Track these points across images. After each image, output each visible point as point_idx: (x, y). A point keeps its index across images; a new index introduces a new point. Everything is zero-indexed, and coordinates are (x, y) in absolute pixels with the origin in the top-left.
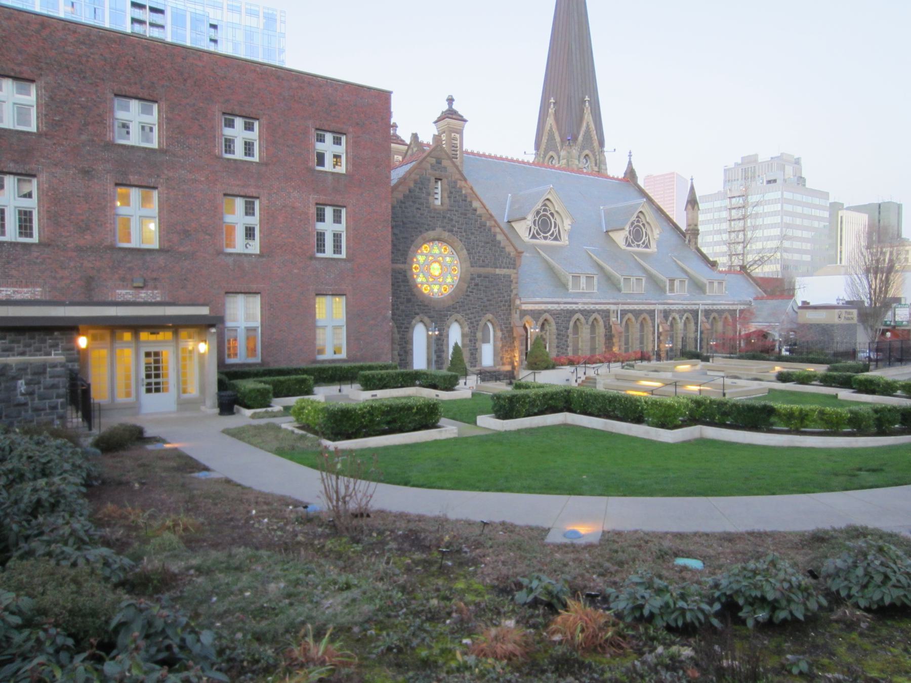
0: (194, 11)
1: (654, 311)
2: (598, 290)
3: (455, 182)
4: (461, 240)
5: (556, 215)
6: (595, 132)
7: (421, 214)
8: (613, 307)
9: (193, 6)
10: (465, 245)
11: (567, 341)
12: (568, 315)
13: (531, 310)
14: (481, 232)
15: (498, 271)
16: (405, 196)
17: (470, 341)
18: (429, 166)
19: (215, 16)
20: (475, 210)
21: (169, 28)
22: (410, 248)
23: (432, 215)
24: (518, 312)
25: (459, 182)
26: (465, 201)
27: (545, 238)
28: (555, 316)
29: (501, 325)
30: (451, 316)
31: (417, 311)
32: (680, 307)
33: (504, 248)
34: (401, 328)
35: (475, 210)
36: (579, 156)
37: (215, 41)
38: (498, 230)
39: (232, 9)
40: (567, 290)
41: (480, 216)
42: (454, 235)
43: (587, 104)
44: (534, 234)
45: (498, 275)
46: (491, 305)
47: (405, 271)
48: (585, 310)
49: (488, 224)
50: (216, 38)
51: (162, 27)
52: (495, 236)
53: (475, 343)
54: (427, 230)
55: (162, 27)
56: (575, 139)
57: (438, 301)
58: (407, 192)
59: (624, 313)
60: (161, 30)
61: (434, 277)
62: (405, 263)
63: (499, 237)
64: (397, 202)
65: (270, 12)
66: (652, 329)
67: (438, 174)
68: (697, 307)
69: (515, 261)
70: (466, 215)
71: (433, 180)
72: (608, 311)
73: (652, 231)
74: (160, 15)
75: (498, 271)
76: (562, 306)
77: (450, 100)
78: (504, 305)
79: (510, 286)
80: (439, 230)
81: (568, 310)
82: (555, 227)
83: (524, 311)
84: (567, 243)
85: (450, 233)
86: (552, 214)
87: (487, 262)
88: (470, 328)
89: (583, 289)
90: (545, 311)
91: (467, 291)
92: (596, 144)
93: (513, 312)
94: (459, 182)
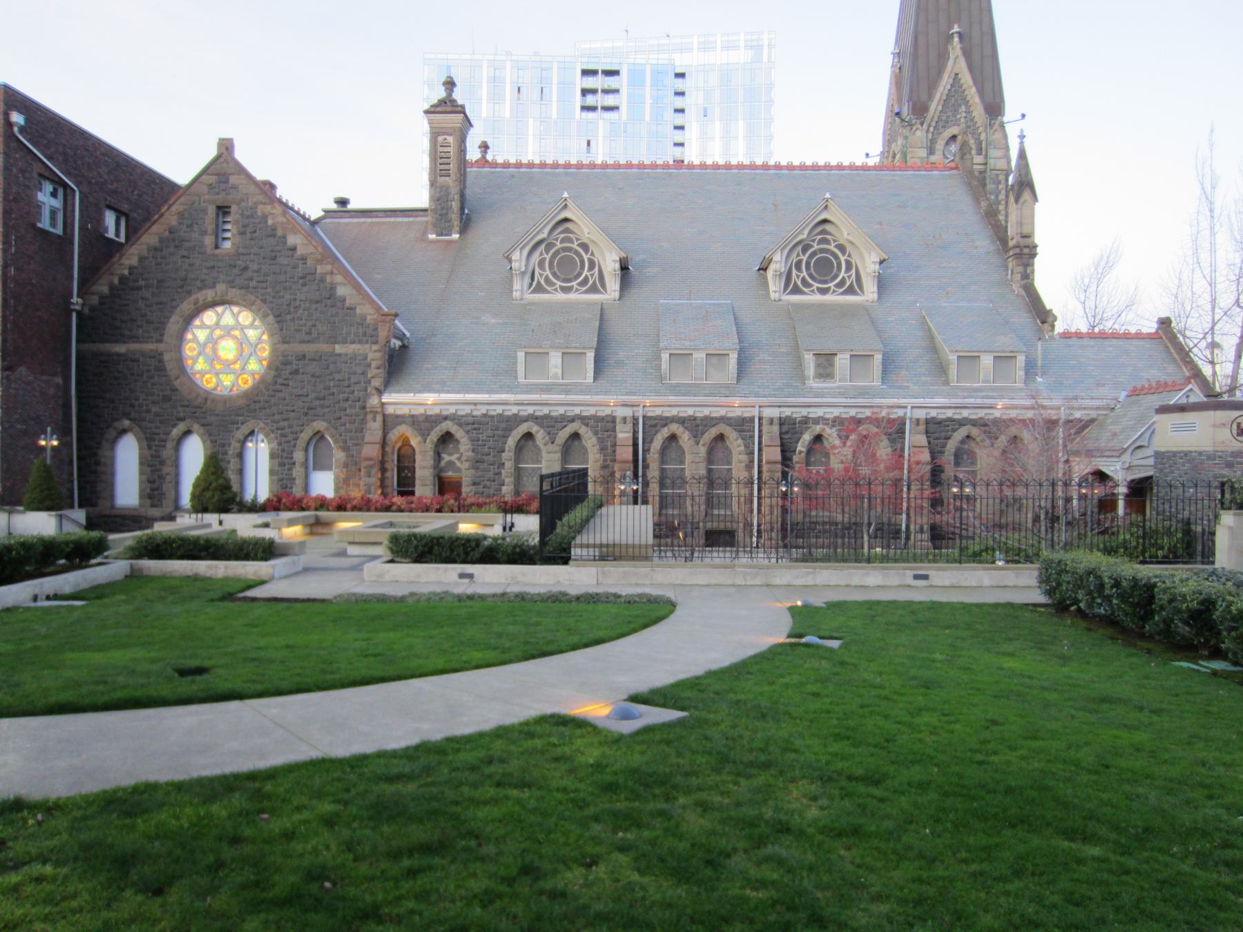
0: (655, 62)
1: (752, 419)
2: (595, 378)
3: (254, 208)
4: (264, 301)
6: (974, 90)
7: (190, 265)
8: (621, 412)
9: (656, 56)
10: (271, 310)
11: (500, 474)
12: (502, 425)
13: (413, 416)
14: (304, 285)
15: (339, 349)
16: (161, 240)
17: (281, 465)
18: (205, 189)
19: (680, 65)
20: (294, 249)
21: (624, 92)
22: (169, 318)
23: (211, 264)
24: (379, 418)
25: (260, 207)
26: (274, 236)
27: (566, 290)
28: (469, 427)
30: (243, 423)
31: (182, 415)
32: (836, 412)
33: (352, 309)
34: (153, 440)
35: (294, 249)
36: (933, 142)
37: (681, 94)
38: (339, 278)
39: (706, 47)
40: (516, 378)
41: (303, 259)
42: (251, 293)
43: (956, 39)
44: (538, 282)
45: (340, 355)
46: (322, 406)
47: (161, 354)
48: (546, 417)
49: (320, 269)
50: (684, 90)
51: (616, 91)
52: (333, 288)
53: (290, 469)
54: (201, 289)
55: (616, 91)
56: (920, 110)
57: (226, 400)
58: (167, 233)
59: (654, 424)
60: (616, 96)
61: (227, 364)
62: (160, 341)
63: (341, 291)
64: (149, 250)
65: (755, 37)
66: (744, 457)
67: (221, 199)
68: (900, 413)
69: (376, 329)
70: (274, 258)
71: (211, 210)
72: (612, 420)
73: (863, 259)
74: (616, 78)
75: (339, 349)
76: (482, 410)
77: (450, 84)
78: (350, 406)
79: (364, 373)
80: (221, 287)
81: (500, 415)
83: (398, 416)
84: (617, 295)
85: (243, 291)
87: (315, 335)
88: (280, 444)
89: (556, 376)
90: (446, 418)
91: (276, 383)
92: (978, 112)
93: (369, 417)
94: (260, 207)
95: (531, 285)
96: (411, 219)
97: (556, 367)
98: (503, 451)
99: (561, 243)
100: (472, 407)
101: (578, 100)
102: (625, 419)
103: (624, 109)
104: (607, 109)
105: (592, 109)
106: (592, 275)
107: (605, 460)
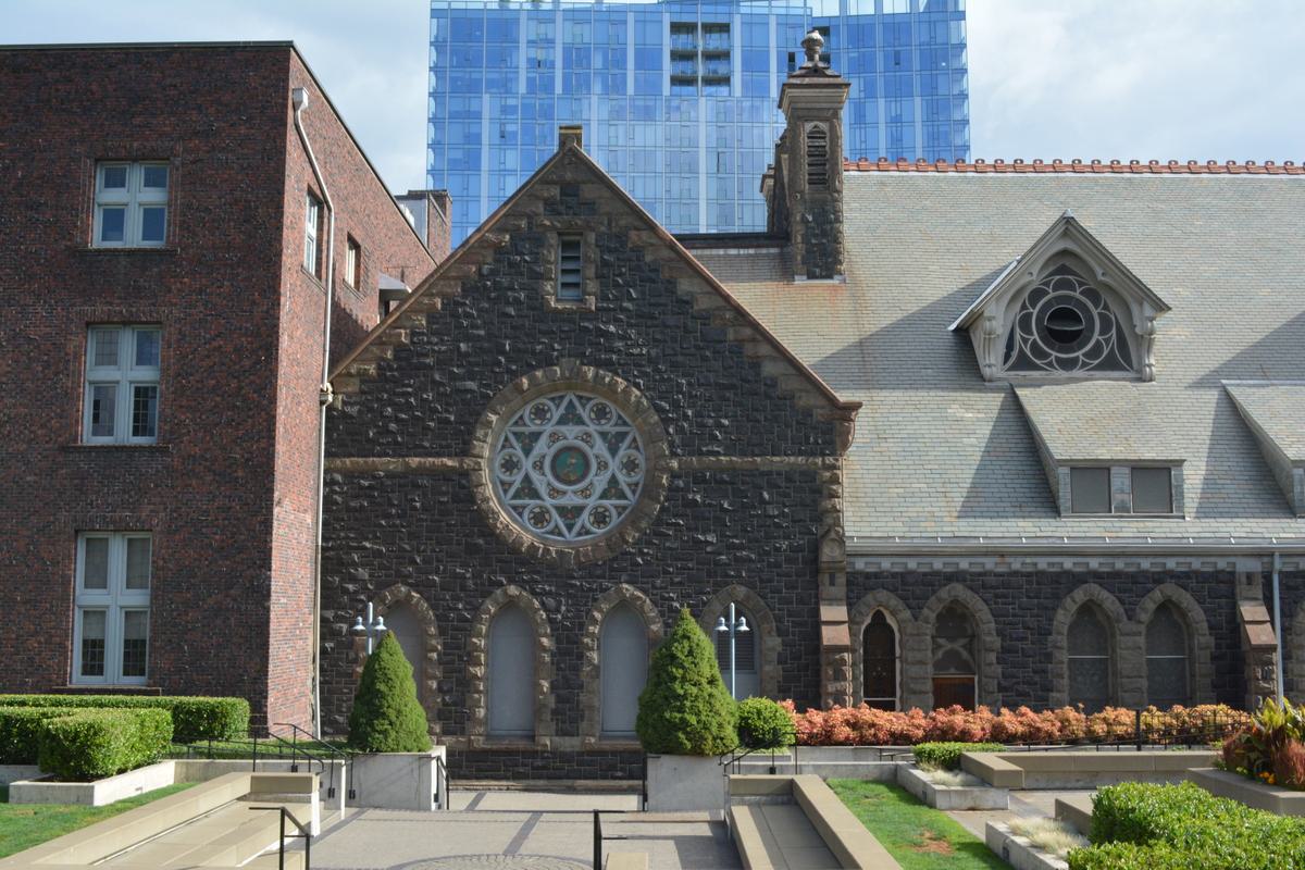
0: (783, 11)
5: (1105, 297)
24: (841, 579)
25: (633, 234)
29: (779, 620)
44: (1021, 350)
82: (1105, 329)
83: (868, 576)
86: (1093, 295)
93: (826, 578)
95: (1007, 357)
96: (751, 251)
97: (1123, 492)
98: (1050, 634)
99: (1054, 290)
100: (998, 560)
101: (668, 68)
102: (1250, 577)
103: (737, 79)
104: (708, 82)
105: (689, 81)
106: (1107, 341)
107: (1218, 646)
